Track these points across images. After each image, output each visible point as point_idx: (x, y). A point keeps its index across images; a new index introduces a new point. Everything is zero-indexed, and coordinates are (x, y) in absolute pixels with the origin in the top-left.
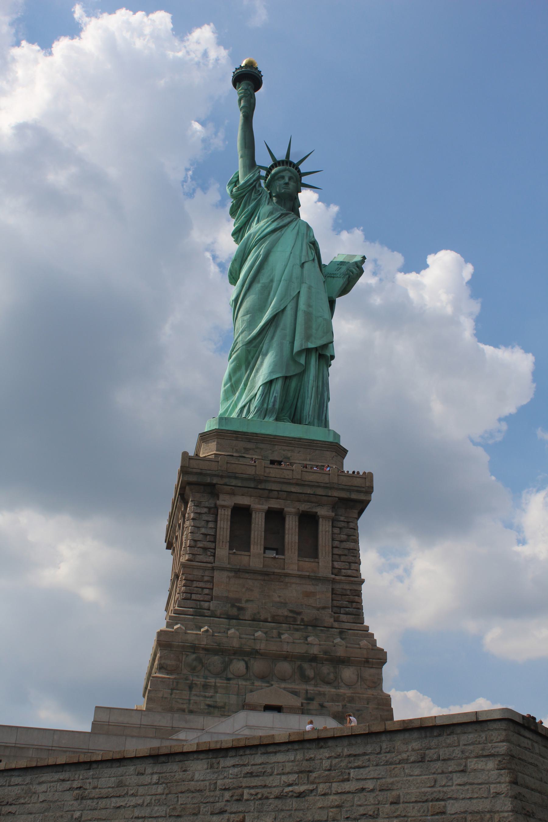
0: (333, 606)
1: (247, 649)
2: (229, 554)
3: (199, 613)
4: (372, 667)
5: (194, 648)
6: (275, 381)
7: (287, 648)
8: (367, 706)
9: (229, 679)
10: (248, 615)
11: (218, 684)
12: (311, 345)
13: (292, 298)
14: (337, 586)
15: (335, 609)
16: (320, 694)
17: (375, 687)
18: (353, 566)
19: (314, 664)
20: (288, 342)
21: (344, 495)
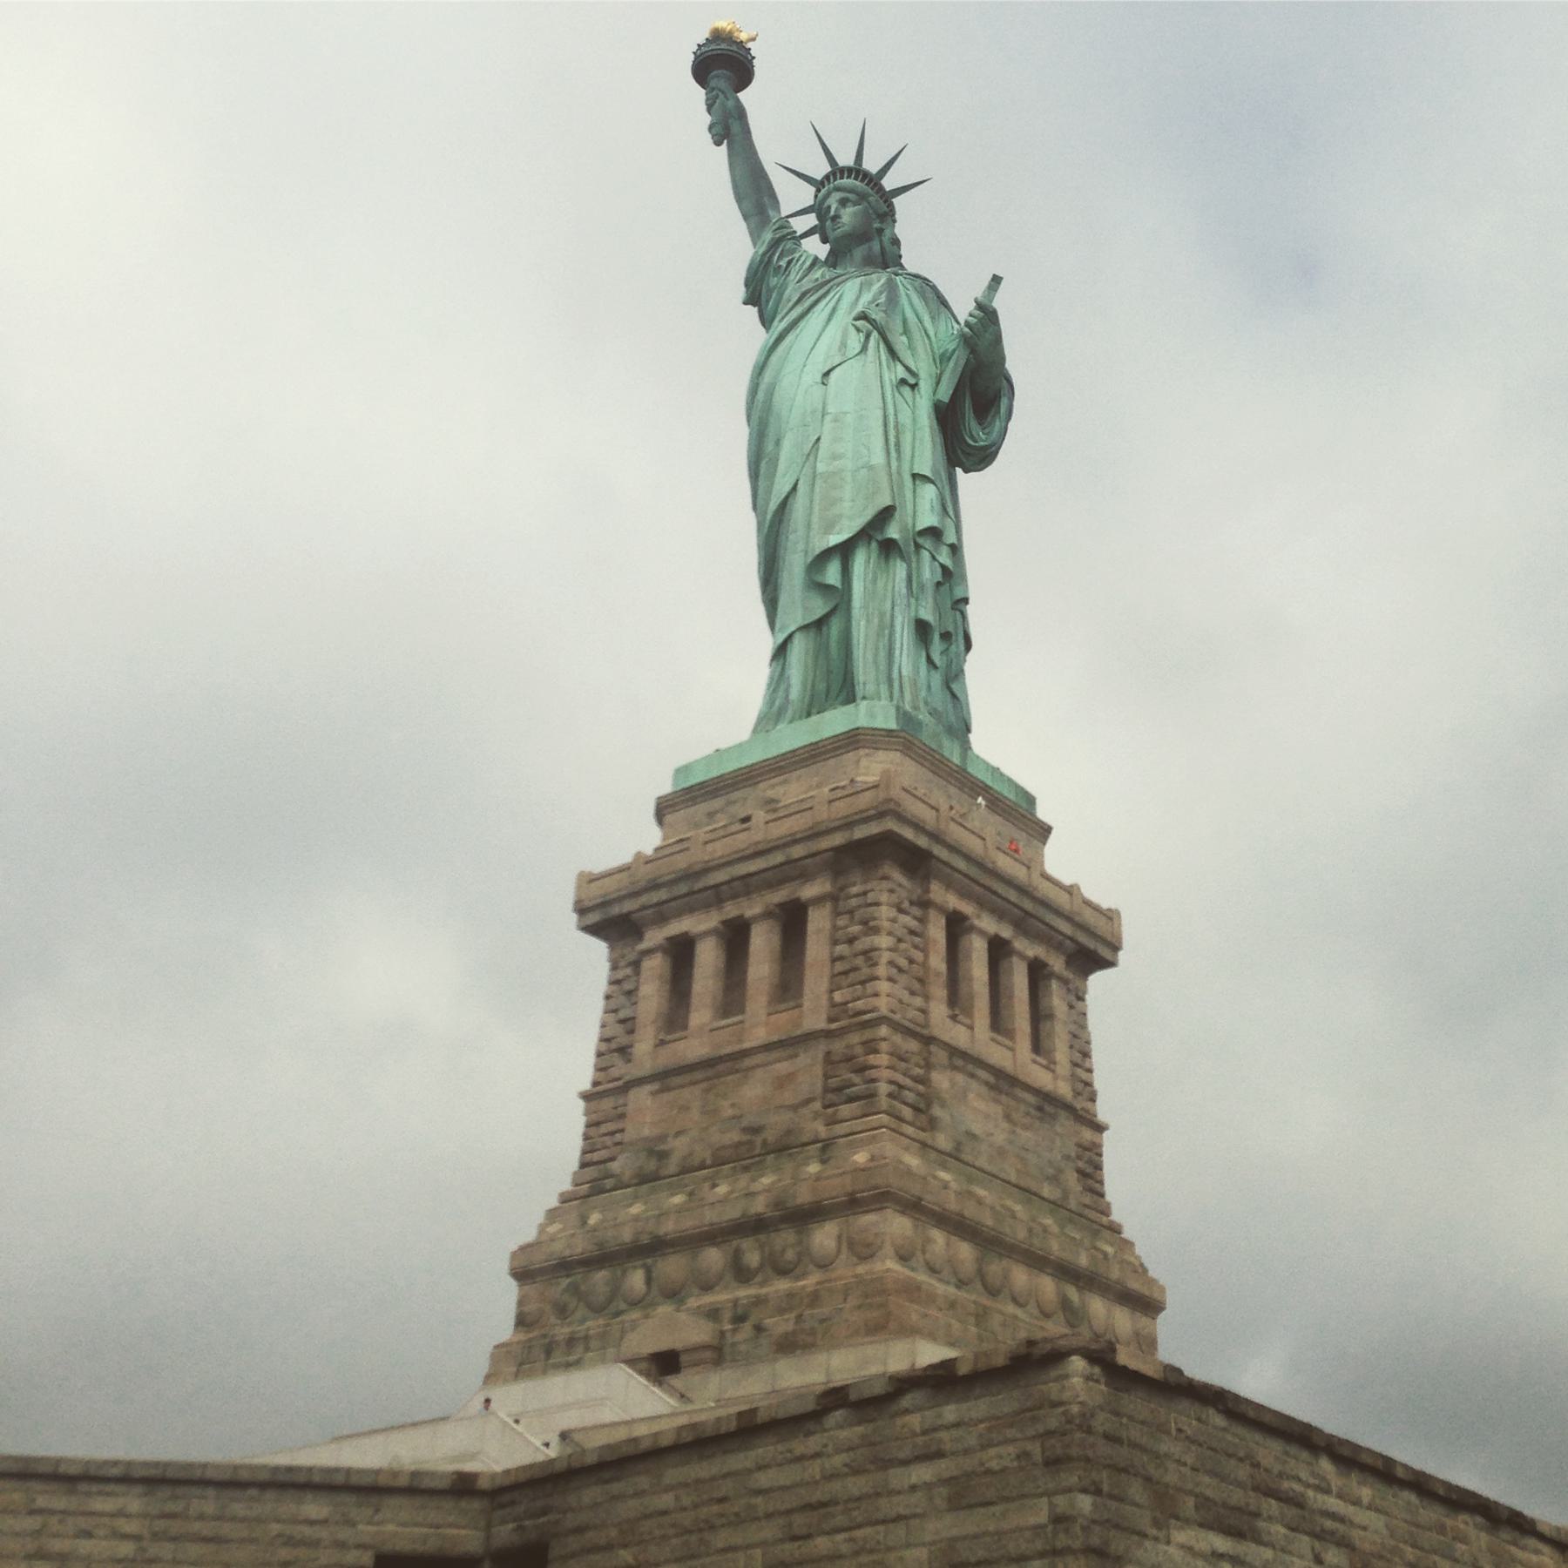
0: (826, 1090)
1: (645, 1240)
5: (565, 1266)
7: (711, 1216)
8: (840, 1306)
9: (618, 1314)
10: (672, 1166)
12: (835, 539)
14: (838, 1046)
15: (832, 1097)
16: (759, 1301)
17: (872, 1256)
18: (870, 987)
19: (762, 1237)
21: (838, 839)
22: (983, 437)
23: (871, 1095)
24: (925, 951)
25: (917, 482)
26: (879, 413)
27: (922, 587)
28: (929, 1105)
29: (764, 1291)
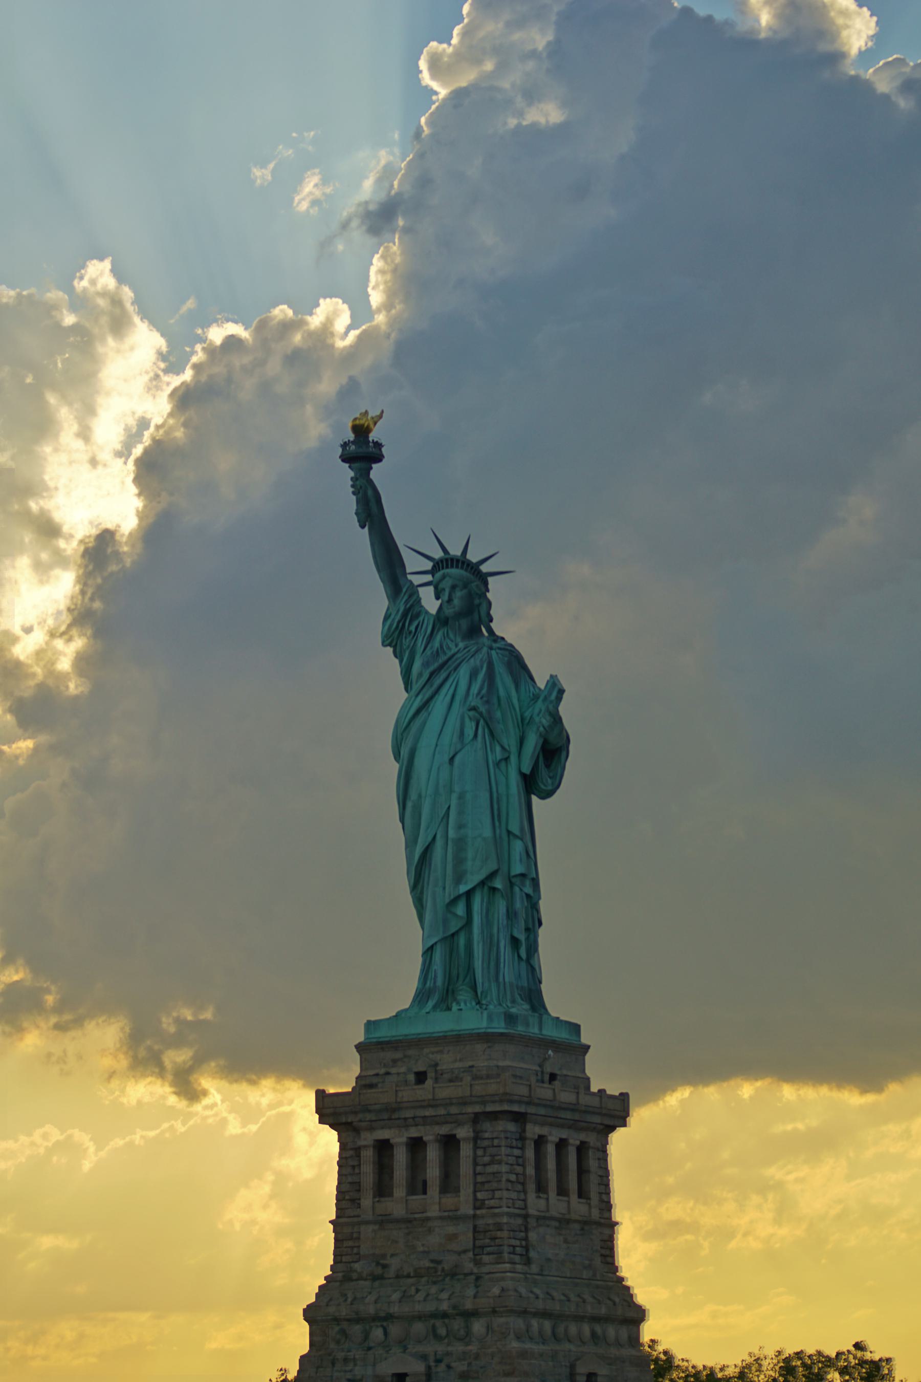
1: (382, 1314)
2: (374, 1203)
3: (347, 1278)
4: (502, 1316)
5: (337, 1320)
6: (434, 948)
7: (419, 1308)
9: (369, 1349)
10: (391, 1272)
11: (357, 1357)
12: (463, 889)
13: (440, 819)
15: (477, 1251)
16: (448, 1354)
17: (505, 1338)
18: (498, 1194)
19: (446, 1321)
20: (441, 889)
21: (478, 1109)
22: (549, 781)
23: (500, 1253)
24: (523, 1166)
25: (511, 837)
26: (487, 795)
27: (516, 914)
28: (527, 1251)
29: (450, 1349)
